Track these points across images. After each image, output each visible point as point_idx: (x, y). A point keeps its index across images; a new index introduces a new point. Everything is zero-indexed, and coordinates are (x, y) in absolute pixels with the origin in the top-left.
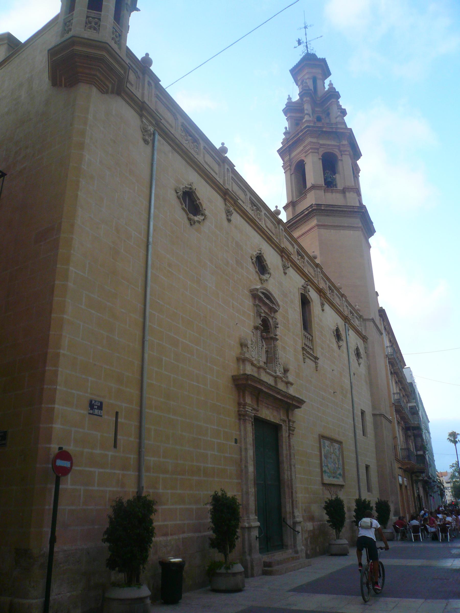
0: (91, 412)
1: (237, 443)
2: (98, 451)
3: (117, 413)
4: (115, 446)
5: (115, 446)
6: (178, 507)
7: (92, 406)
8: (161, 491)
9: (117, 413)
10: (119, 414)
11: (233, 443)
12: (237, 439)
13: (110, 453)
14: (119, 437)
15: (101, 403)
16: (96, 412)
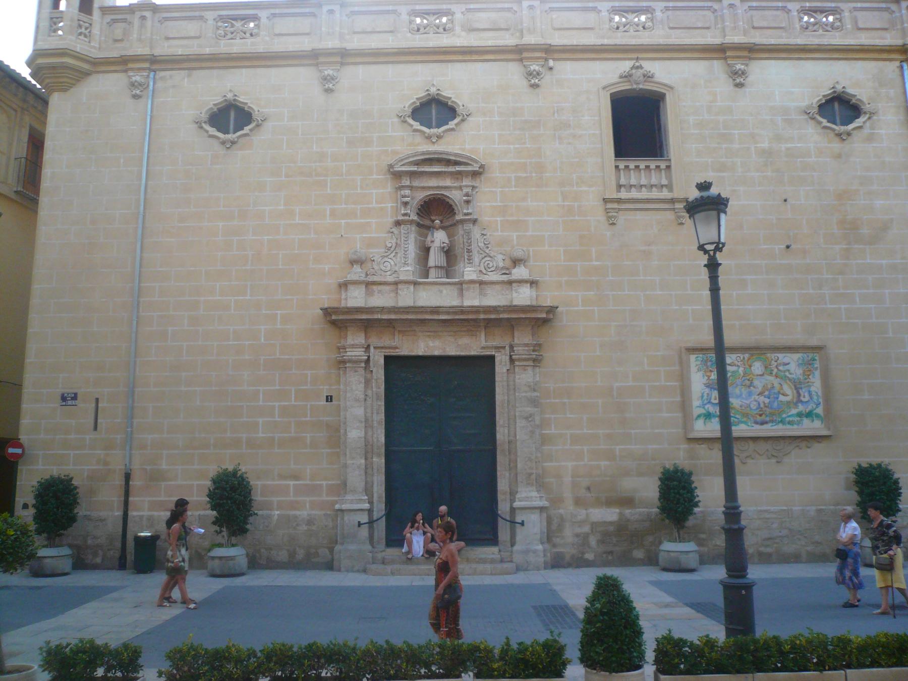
0: (64, 403)
1: (331, 401)
2: (72, 436)
3: (97, 400)
4: (96, 428)
5: (96, 428)
6: (196, 483)
7: (64, 398)
8: (164, 467)
9: (97, 400)
10: (100, 400)
11: (324, 402)
12: (331, 397)
13: (87, 437)
14: (99, 421)
15: (76, 394)
16: (70, 403)
